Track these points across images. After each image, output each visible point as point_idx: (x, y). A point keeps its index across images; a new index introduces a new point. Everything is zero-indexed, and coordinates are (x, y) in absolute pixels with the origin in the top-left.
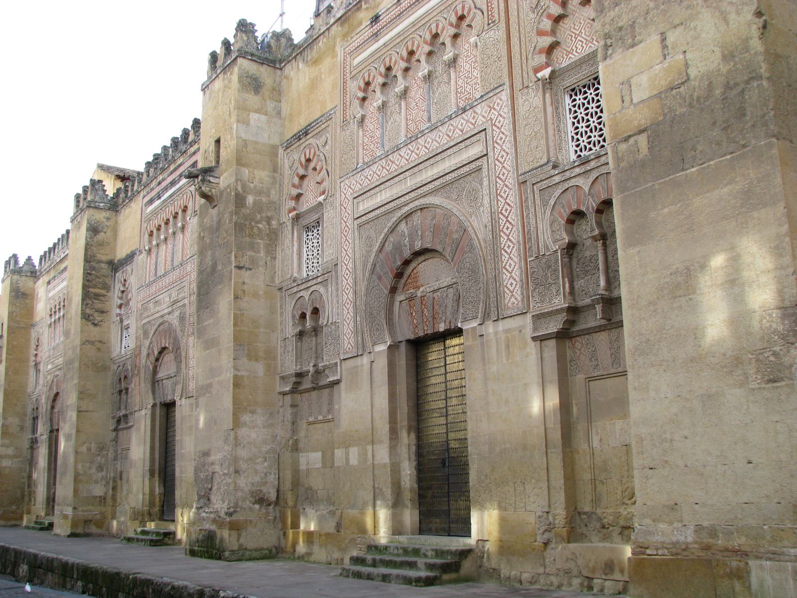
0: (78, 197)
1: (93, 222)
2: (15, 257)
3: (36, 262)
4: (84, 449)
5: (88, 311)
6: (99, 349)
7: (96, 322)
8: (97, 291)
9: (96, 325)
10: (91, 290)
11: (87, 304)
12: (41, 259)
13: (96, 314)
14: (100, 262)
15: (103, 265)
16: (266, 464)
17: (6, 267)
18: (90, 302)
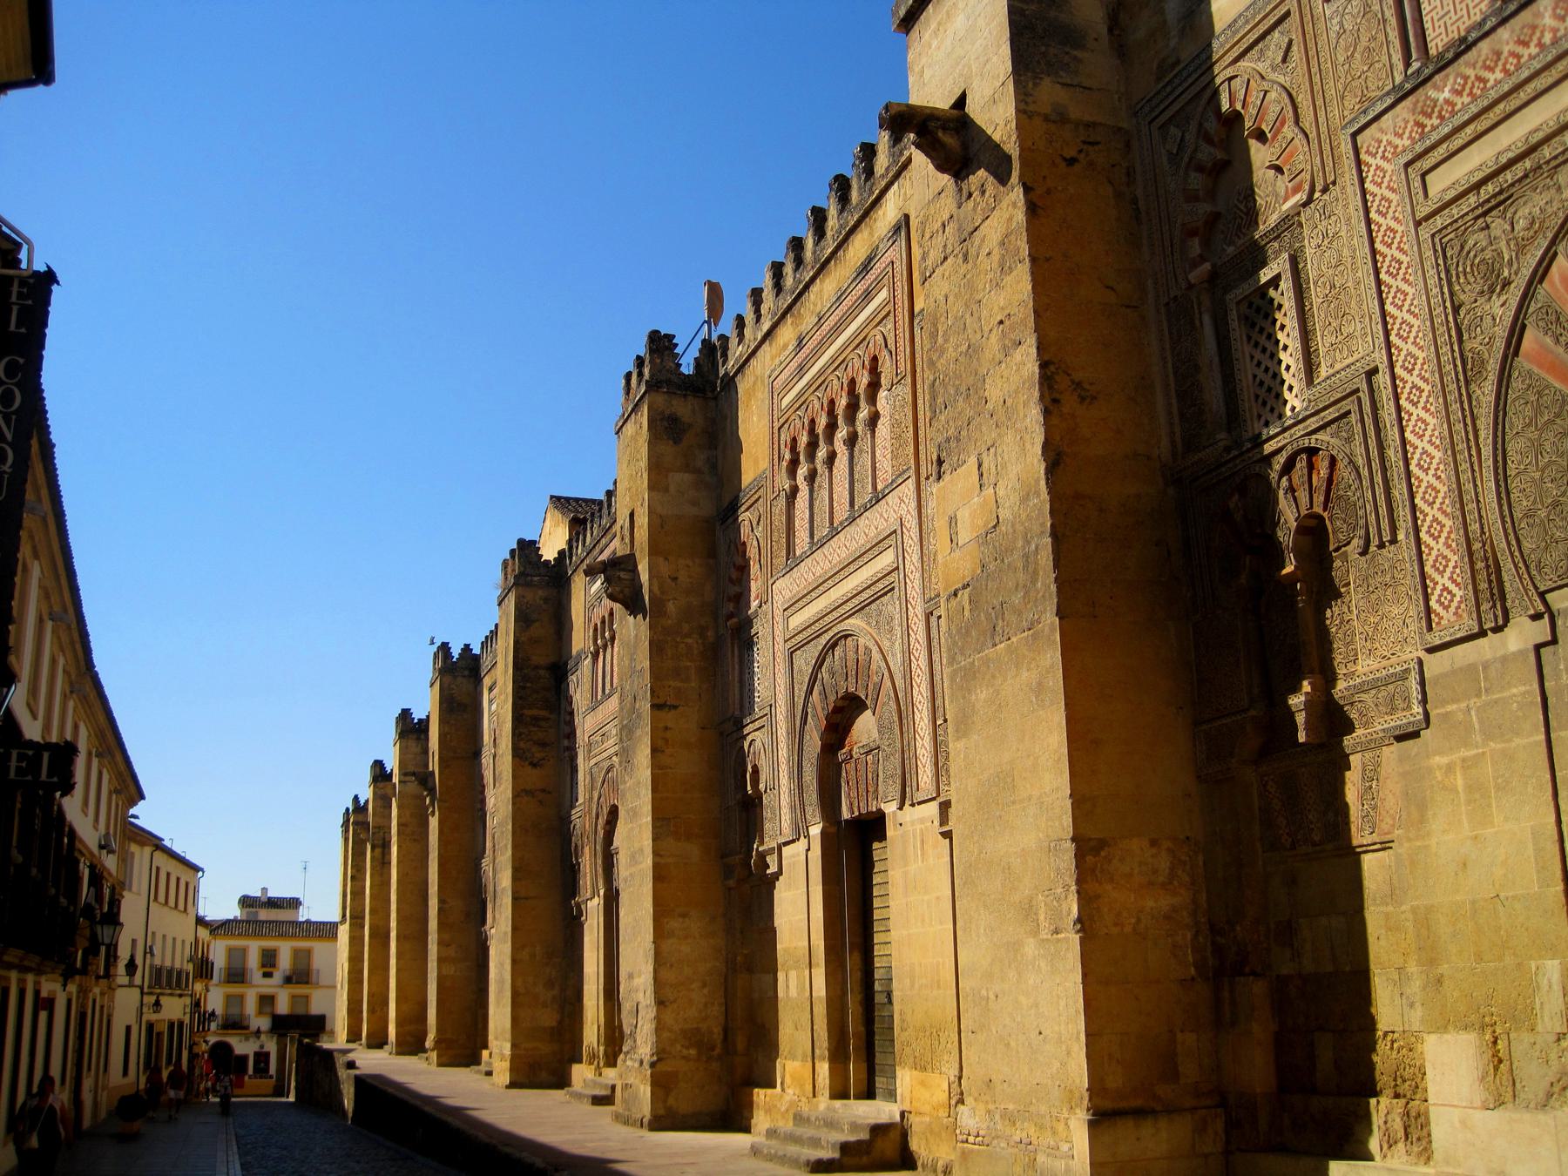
0: (505, 563)
1: (524, 607)
2: (445, 647)
3: (476, 650)
4: (525, 955)
5: (522, 745)
6: (540, 802)
7: (535, 761)
8: (535, 712)
9: (534, 765)
10: (528, 712)
11: (520, 734)
12: (482, 648)
13: (535, 749)
14: (537, 667)
15: (542, 672)
16: (706, 991)
17: (435, 664)
18: (525, 731)
